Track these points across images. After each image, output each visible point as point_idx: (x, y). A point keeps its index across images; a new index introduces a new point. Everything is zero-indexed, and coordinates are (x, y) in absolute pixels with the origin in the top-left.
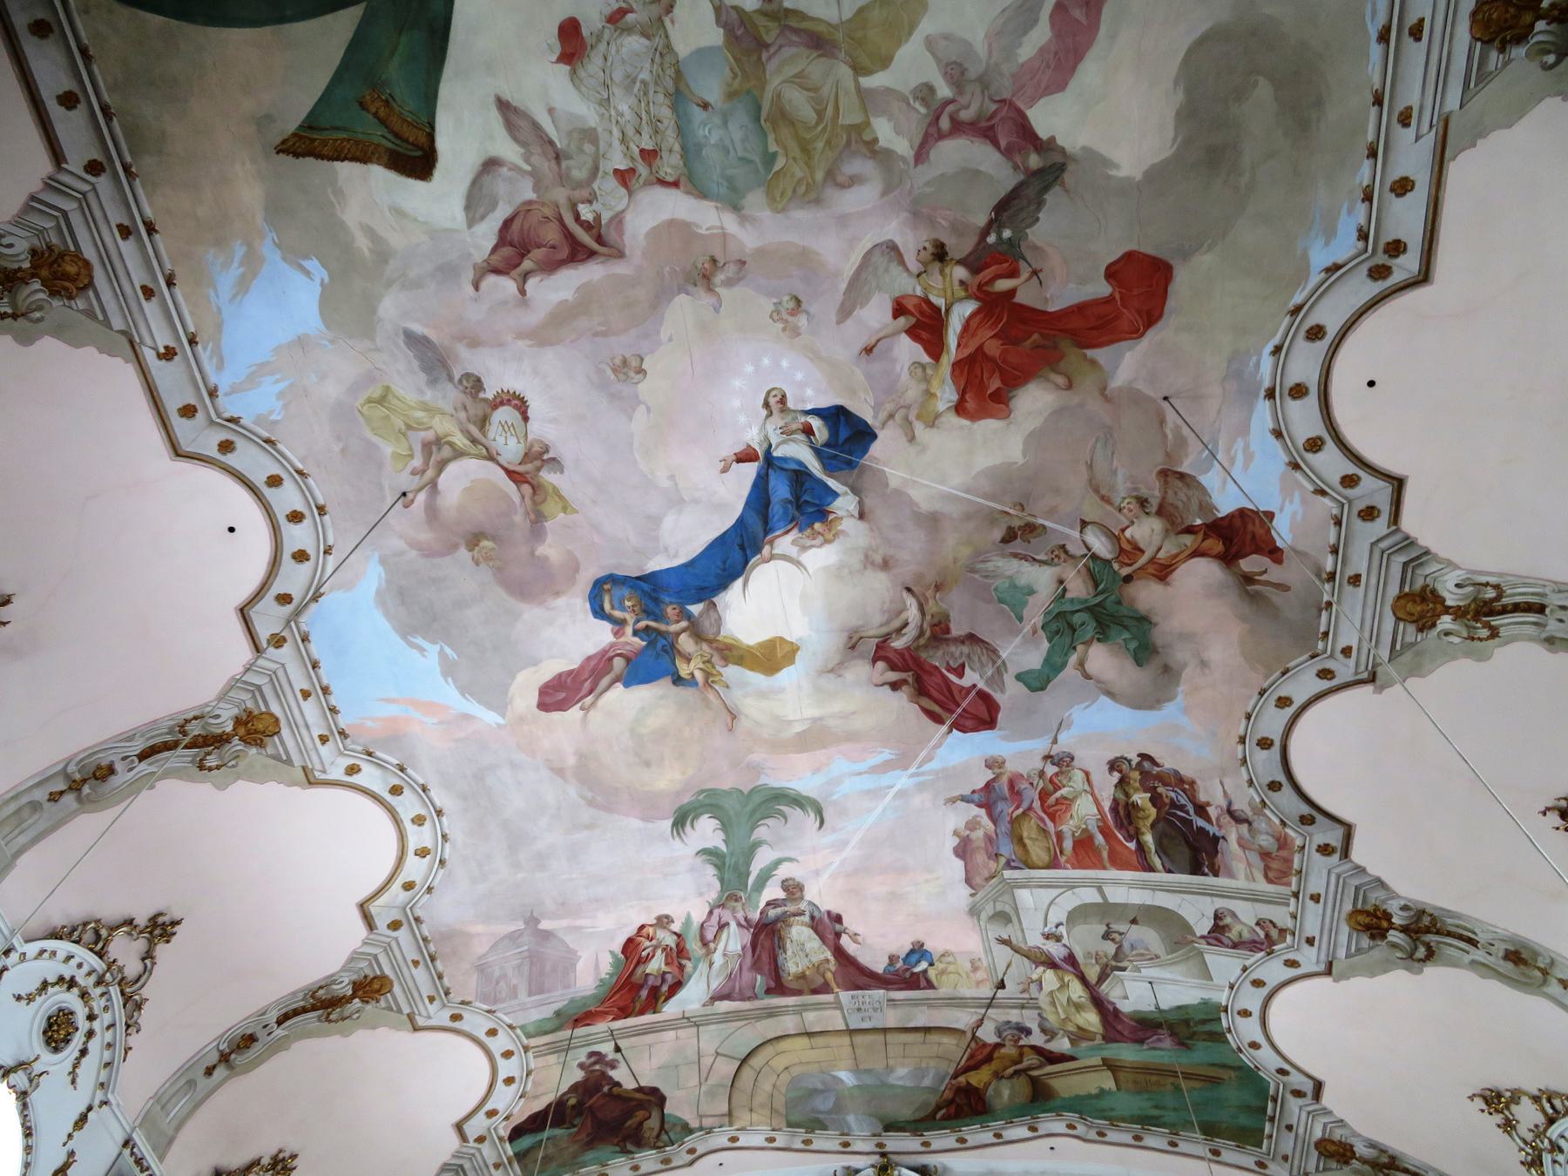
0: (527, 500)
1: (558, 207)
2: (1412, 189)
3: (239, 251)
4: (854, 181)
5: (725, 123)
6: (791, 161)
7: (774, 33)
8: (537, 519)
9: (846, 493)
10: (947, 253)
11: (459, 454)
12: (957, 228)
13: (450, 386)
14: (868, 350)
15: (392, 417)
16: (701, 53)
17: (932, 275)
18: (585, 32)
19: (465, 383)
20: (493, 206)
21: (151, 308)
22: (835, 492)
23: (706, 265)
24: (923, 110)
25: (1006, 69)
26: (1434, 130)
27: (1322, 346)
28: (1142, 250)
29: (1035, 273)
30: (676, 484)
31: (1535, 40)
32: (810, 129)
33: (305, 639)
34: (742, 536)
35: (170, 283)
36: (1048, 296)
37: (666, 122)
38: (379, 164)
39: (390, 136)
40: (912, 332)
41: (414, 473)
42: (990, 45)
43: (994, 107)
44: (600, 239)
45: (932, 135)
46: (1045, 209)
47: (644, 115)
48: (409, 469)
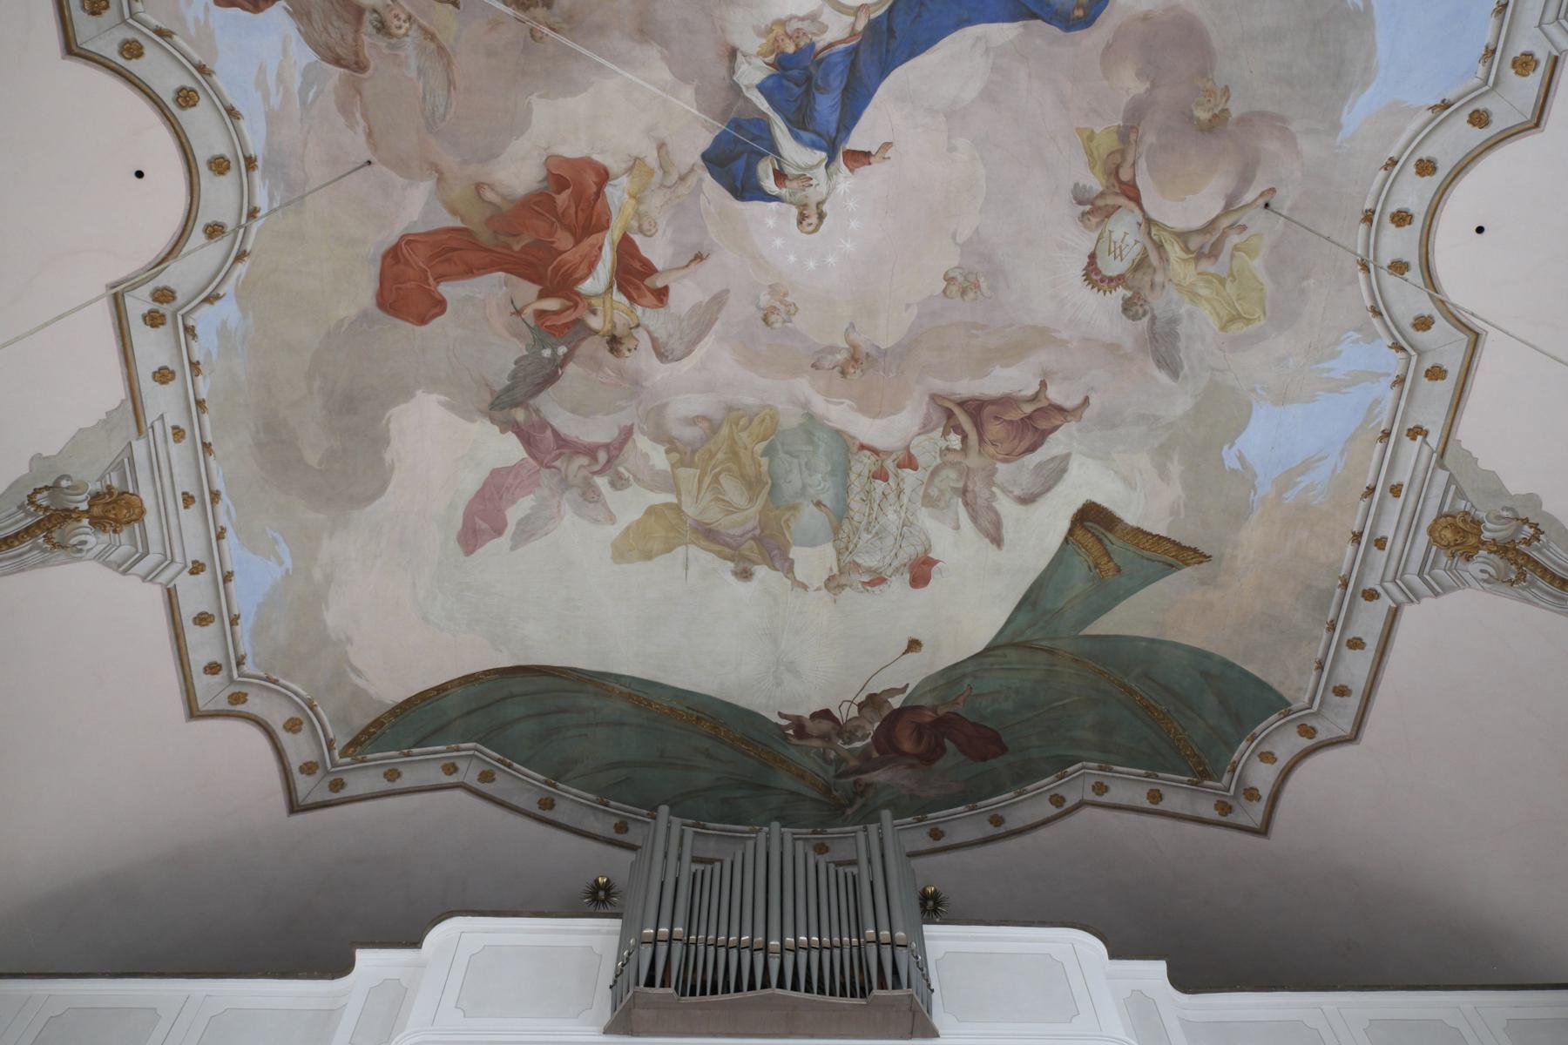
0: (1130, 160)
1: (980, 451)
2: (154, 373)
3: (1290, 496)
4: (693, 421)
5: (804, 487)
6: (750, 447)
7: (747, 546)
8: (1127, 133)
9: (748, 87)
10: (608, 343)
11: (1183, 236)
12: (599, 365)
13: (1156, 312)
14: (699, 257)
15: (1234, 298)
16: (813, 543)
17: (624, 324)
18: (907, 576)
19: (1141, 311)
20: (1040, 466)
21: (1403, 476)
22: (761, 92)
23: (852, 370)
24: (621, 469)
25: (546, 492)
26: (149, 426)
27: (204, 219)
28: (408, 326)
29: (518, 312)
30: (949, 138)
31: (83, 497)
32: (729, 470)
33: (1490, 52)
34: (888, 51)
36: (504, 288)
37: (857, 498)
38: (1126, 524)
39: (1106, 541)
40: (649, 269)
41: (1244, 228)
42: (559, 511)
43: (557, 463)
44: (950, 415)
45: (615, 448)
46: (509, 372)
48: (1245, 235)
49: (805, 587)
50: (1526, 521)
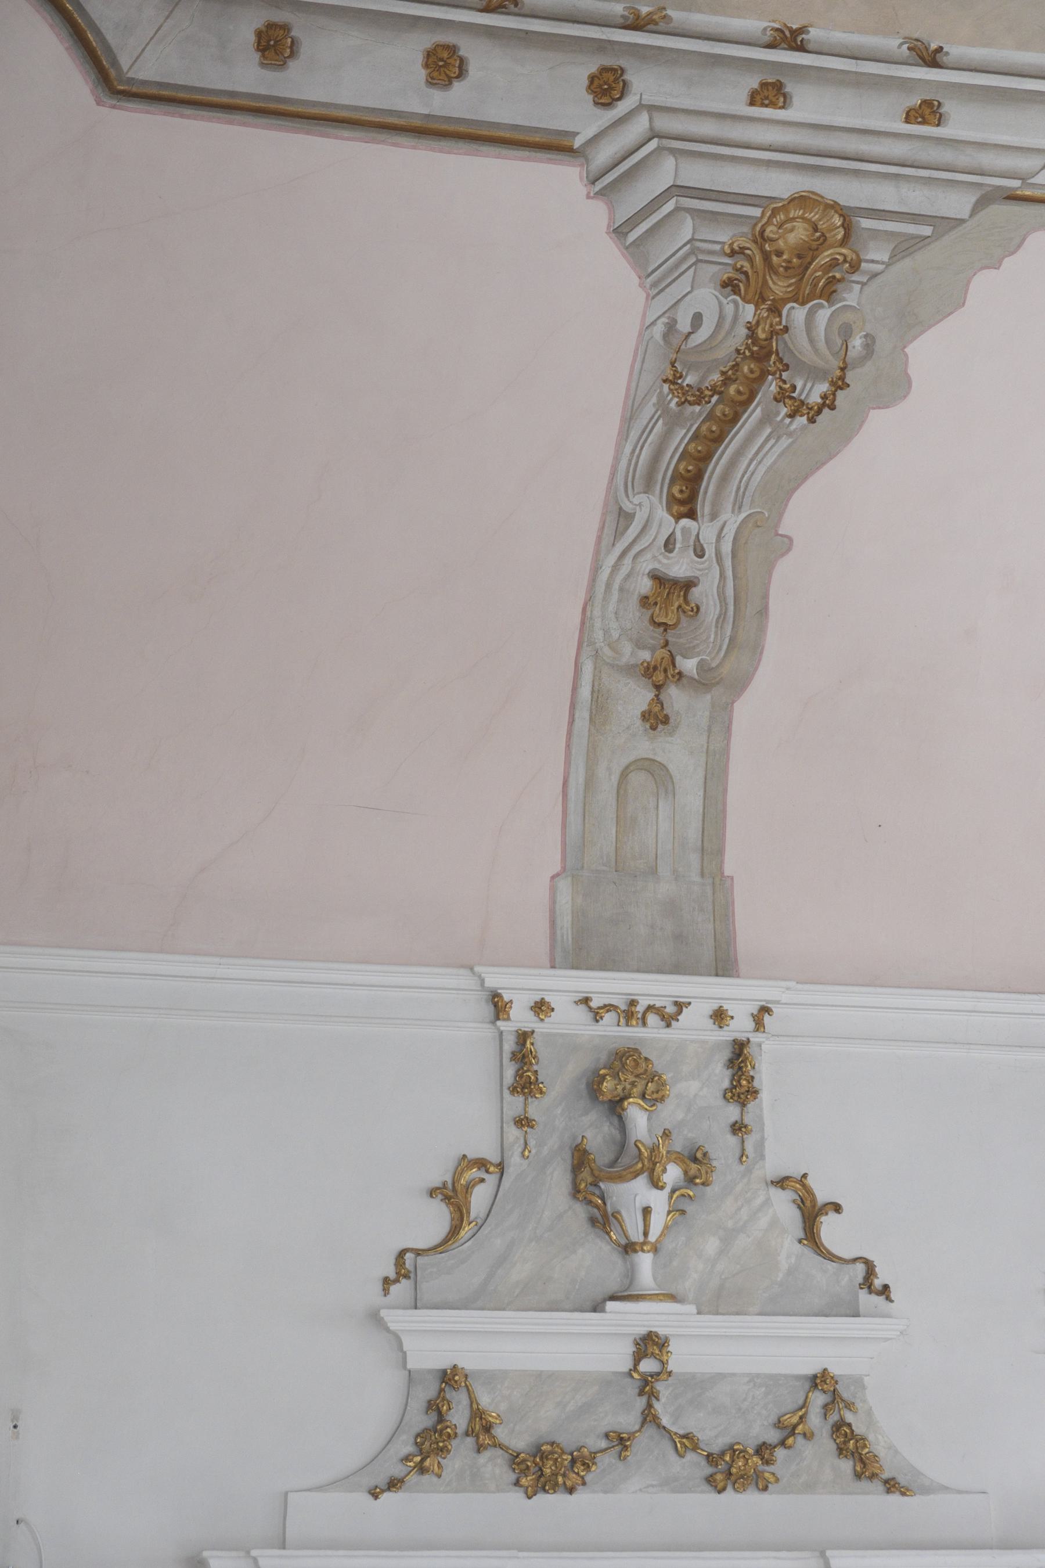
35: (932, 59)
50: (840, 384)
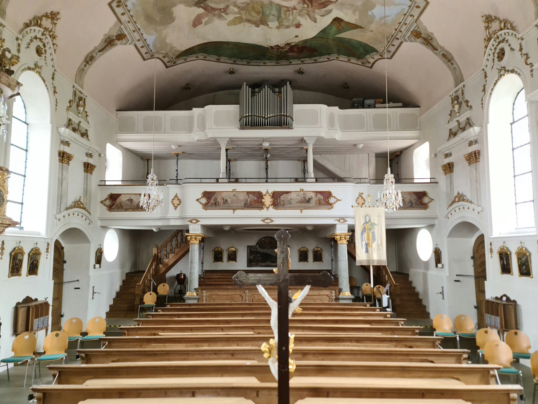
16: (273, 21)
20: (326, 11)
21: (408, 22)
24: (227, 12)
25: (210, 17)
35: (400, 23)
47: (287, 16)
49: (271, 28)
50: (430, 36)
